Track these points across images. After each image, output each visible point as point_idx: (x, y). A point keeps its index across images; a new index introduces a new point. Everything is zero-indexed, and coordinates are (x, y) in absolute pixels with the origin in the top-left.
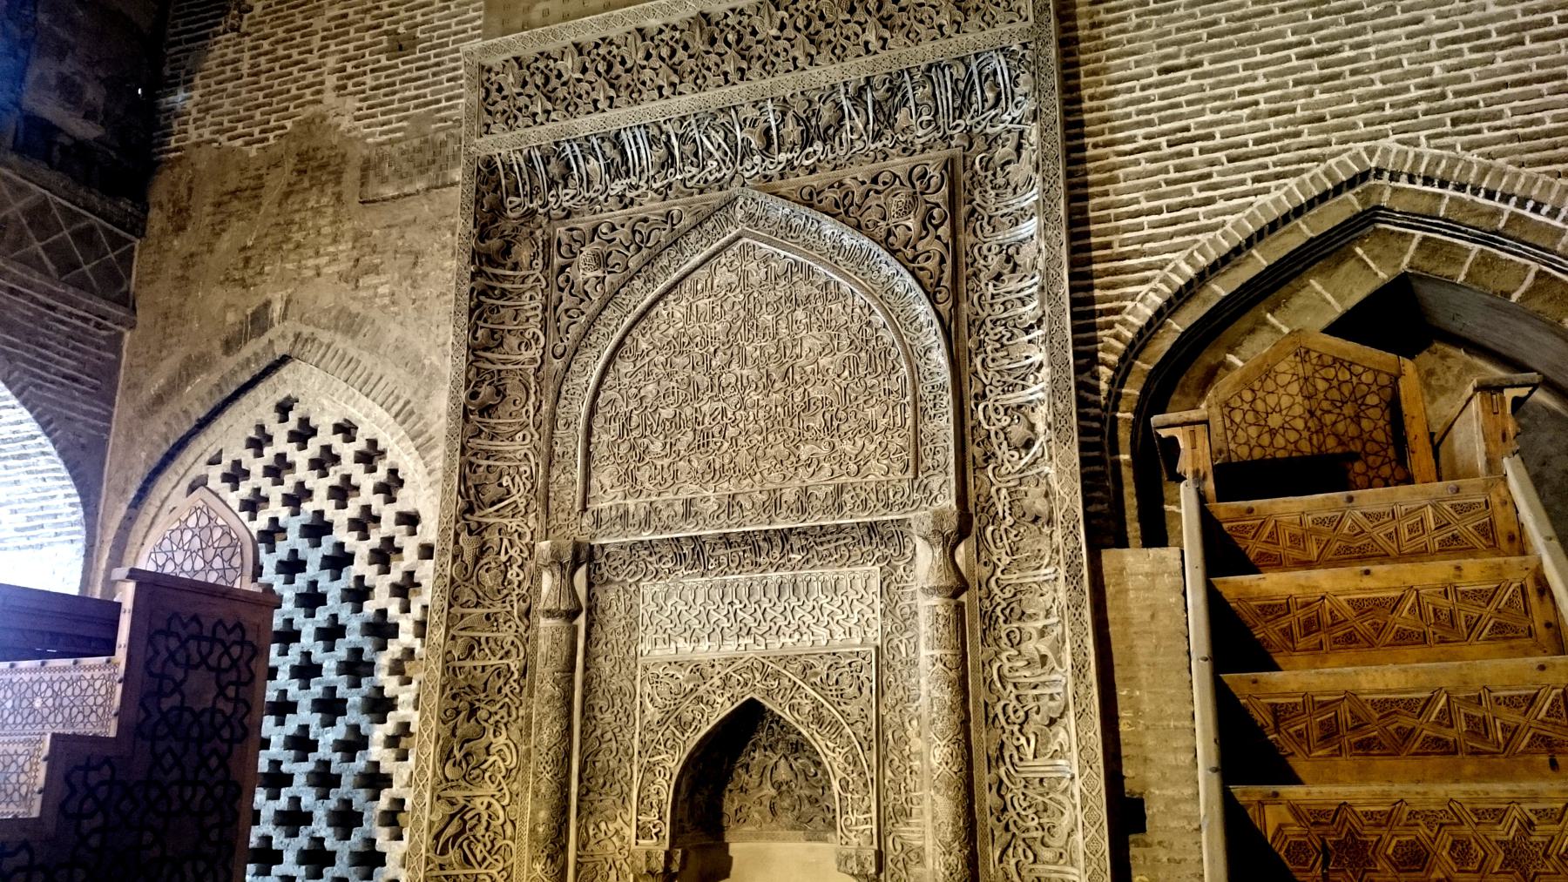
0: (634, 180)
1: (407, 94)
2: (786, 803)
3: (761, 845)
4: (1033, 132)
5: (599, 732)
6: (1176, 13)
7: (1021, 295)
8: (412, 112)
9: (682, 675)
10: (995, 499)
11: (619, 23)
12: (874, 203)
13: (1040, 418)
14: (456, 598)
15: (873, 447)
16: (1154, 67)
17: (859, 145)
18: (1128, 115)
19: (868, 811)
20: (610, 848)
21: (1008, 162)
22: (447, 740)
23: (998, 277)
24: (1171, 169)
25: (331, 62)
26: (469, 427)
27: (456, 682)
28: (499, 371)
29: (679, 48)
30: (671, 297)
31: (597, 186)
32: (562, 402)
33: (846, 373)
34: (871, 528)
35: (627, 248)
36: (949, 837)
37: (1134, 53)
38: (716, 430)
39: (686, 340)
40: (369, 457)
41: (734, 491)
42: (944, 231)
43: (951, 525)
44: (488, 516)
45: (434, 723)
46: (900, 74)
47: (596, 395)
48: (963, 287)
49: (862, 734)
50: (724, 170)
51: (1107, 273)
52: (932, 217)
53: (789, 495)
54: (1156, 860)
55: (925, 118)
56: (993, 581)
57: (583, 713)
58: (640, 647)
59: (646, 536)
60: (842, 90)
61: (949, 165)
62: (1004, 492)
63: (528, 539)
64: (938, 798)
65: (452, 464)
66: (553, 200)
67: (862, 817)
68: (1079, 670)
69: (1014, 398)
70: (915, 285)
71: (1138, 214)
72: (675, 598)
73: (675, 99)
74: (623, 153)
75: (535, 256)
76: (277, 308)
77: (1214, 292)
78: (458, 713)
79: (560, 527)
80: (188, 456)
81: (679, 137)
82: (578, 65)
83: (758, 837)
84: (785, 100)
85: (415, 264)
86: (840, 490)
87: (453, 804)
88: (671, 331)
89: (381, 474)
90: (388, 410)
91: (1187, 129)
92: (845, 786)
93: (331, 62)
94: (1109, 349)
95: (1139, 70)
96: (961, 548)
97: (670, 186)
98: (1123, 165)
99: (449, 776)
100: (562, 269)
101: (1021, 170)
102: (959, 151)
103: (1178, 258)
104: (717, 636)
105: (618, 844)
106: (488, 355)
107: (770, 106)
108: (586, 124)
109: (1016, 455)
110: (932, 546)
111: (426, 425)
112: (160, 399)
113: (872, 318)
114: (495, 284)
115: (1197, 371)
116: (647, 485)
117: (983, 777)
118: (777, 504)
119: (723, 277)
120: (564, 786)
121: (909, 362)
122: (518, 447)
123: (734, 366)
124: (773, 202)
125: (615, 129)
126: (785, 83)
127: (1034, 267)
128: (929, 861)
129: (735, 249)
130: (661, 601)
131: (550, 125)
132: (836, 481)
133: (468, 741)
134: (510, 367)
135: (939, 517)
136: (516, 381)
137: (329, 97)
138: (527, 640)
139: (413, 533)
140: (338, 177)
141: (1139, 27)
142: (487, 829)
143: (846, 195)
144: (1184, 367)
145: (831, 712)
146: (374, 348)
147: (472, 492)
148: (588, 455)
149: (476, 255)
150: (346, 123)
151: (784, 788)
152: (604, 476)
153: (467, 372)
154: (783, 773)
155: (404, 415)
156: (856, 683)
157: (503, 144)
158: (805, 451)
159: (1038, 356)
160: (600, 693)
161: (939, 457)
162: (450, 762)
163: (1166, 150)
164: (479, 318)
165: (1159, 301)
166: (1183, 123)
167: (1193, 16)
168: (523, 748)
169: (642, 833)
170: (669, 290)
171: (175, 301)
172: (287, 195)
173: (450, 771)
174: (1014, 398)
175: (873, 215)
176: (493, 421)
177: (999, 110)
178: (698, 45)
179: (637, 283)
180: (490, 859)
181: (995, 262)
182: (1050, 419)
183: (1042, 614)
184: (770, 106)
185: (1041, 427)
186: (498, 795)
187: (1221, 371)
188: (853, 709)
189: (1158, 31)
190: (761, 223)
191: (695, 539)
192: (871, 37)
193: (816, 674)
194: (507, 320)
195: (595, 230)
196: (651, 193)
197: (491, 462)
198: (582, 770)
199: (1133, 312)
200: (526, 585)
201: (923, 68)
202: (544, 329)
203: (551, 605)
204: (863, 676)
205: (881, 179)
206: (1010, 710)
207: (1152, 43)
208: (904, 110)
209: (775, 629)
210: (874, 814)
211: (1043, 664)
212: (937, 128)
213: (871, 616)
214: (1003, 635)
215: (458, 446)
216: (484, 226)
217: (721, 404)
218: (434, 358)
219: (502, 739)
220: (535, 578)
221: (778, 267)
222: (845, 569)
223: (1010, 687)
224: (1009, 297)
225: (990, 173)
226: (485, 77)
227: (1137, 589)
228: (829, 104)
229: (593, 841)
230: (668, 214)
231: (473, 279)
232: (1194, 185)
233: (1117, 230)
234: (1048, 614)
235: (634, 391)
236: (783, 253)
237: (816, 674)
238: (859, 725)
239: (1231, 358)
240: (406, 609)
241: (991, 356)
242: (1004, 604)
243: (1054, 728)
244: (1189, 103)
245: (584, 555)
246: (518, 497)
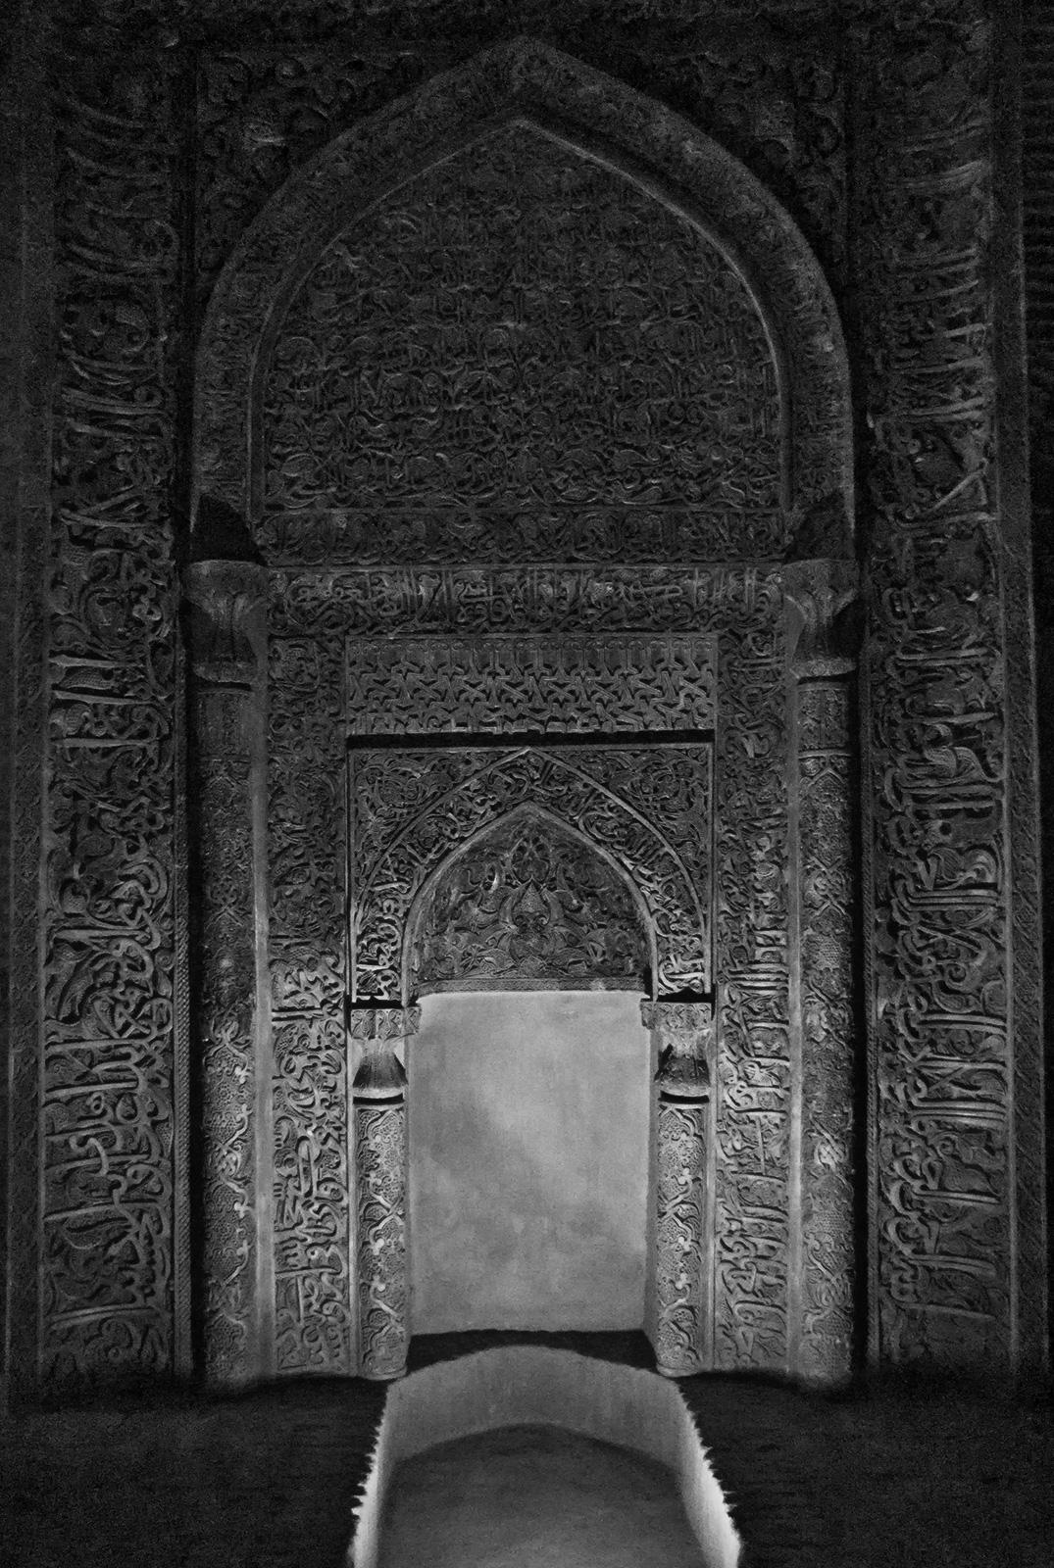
67: (689, 964)
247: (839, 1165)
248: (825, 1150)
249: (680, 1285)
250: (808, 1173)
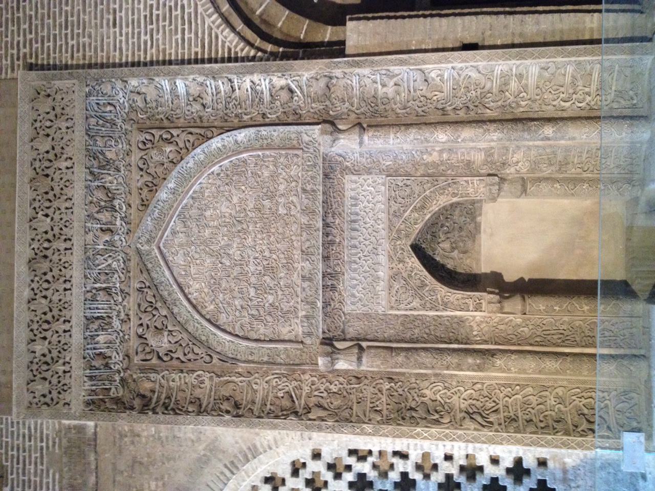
0: (115, 313)
1: (32, 471)
2: (461, 244)
3: (483, 259)
4: (134, 82)
5: (425, 336)
6: (87, 20)
7: (215, 94)
8: (44, 468)
9: (396, 286)
10: (316, 110)
11: (21, 314)
12: (154, 170)
13: (279, 82)
14: (347, 420)
15: (284, 174)
16: (112, 30)
17: (120, 180)
18: (133, 43)
19: (467, 182)
20: (486, 329)
21: (145, 100)
22: (429, 422)
23: (204, 106)
24: (164, 24)
26: (246, 415)
27: (395, 418)
28: (215, 400)
29: (44, 278)
30: (186, 291)
31: (114, 337)
32: (239, 357)
33: (243, 188)
34: (326, 176)
35: (154, 316)
36: (481, 130)
37: (103, 40)
38: (265, 263)
39: (212, 281)
41: (299, 252)
42: (175, 132)
43: (328, 127)
44: (300, 405)
45: (419, 429)
46: (87, 150)
47: (237, 336)
48: (206, 124)
49: (429, 185)
50: (120, 258)
51: (210, 50)
52: (166, 139)
53: (304, 220)
54: (490, 36)
55: (113, 143)
56: (357, 111)
57: (414, 343)
58: (380, 312)
59: (320, 304)
60: (89, 183)
61: (140, 130)
62: (313, 105)
63: (315, 379)
64: (462, 137)
65: (268, 424)
66: (117, 367)
67: (471, 185)
68: (402, 63)
69: (267, 97)
70: (201, 147)
71: (183, 39)
72: (355, 291)
73: (73, 280)
74: (98, 318)
75: (148, 379)
77: (226, 10)
78: (413, 417)
79: (311, 357)
81: (96, 282)
82: (41, 341)
83: (478, 261)
84: (88, 216)
85: (141, 463)
86: (304, 191)
87: (464, 418)
88: (206, 290)
90: (228, 480)
91: (145, 16)
92: (455, 195)
94: (249, 52)
95: (112, 38)
96: (340, 127)
97: (122, 291)
98: (158, 46)
99: (448, 420)
100: (159, 358)
101: (151, 94)
102: (135, 126)
103: (208, 21)
104: (376, 267)
105: (484, 325)
106: (204, 406)
107: (89, 225)
108: (77, 337)
109: (296, 98)
110: (338, 139)
111: (240, 452)
113: (215, 173)
114: (161, 403)
115: (263, 27)
116: (291, 304)
117: (452, 117)
118: (309, 227)
119: (179, 260)
120: (454, 350)
121: (241, 153)
123: (231, 252)
124: (142, 227)
125: (83, 319)
126: (79, 212)
127: (202, 84)
128: (493, 144)
129: (165, 251)
130: (356, 300)
131: (73, 362)
132: (300, 193)
133: (429, 411)
134: (213, 393)
135: (323, 132)
136: (222, 389)
138: (373, 377)
139: (304, 465)
141: (90, 37)
142: (478, 400)
143: (147, 186)
145: (417, 203)
147: (285, 413)
148: (271, 341)
149: (142, 411)
151: (454, 245)
152: (285, 331)
153: (213, 415)
154: (446, 245)
156: (404, 188)
157: (79, 390)
158: (282, 211)
159: (248, 84)
160: (404, 336)
161: (293, 136)
162: (440, 420)
163: (154, 26)
164: (181, 410)
165: (227, 30)
166: (142, 18)
167: (90, 12)
168: (433, 379)
169: (478, 308)
170: (182, 291)
173: (446, 420)
174: (267, 97)
175: (160, 170)
176: (244, 402)
177: (117, 105)
178: (45, 266)
179: (176, 310)
180: (494, 399)
181: (197, 107)
182: (280, 74)
183: (375, 85)
184: (89, 225)
185: (283, 82)
186: (459, 394)
187: (264, 17)
188: (417, 189)
189: (94, 28)
190: (153, 235)
191: (324, 276)
192: (64, 165)
193: (399, 209)
194: (184, 396)
195: (140, 337)
196: (125, 303)
197: (269, 403)
198: (446, 343)
199: (231, 42)
200: (341, 379)
201: (87, 138)
202: (193, 371)
203: (354, 358)
204: (400, 184)
205: (142, 166)
206: (420, 104)
207: (100, 30)
208: (107, 153)
209: (375, 233)
210: (469, 178)
211: (399, 85)
212: (120, 137)
213: (370, 181)
214: (384, 107)
215: (257, 420)
216: (125, 408)
217: (251, 260)
218: (201, 448)
219: (427, 392)
220: (339, 373)
222: (346, 194)
223: (410, 104)
224: (215, 101)
225: (149, 110)
226: (34, 406)
227: (365, 40)
228: (95, 192)
229: (484, 338)
230: (140, 290)
231: (157, 413)
232: (174, 13)
233: (190, 49)
234: (375, 82)
235: (237, 313)
236: (172, 223)
237: (399, 209)
238: (425, 186)
239: (258, 13)
240: (349, 468)
241: (244, 110)
242: (369, 107)
243: (430, 80)
244: (133, 14)
245: (328, 341)
246: (291, 386)
247: (553, 127)
248: (546, 132)
249: (603, 188)
250: (556, 139)
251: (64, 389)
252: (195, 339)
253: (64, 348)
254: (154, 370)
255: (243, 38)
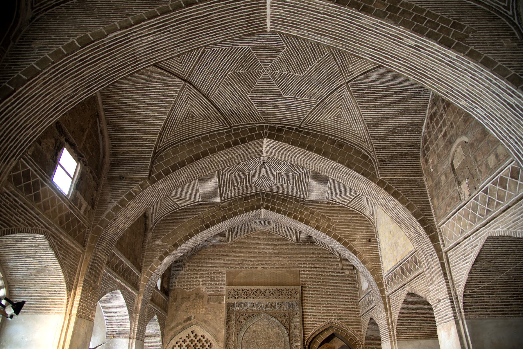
25: (201, 280)
40: (207, 341)
61: (289, 313)
69: (296, 344)
76: (193, 317)
80: (176, 337)
89: (209, 344)
93: (201, 280)
101: (297, 316)
108: (243, 300)
112: (173, 328)
115: (313, 341)
122: (232, 343)
137: (201, 286)
140: (202, 299)
144: (313, 341)
146: (209, 326)
150: (204, 290)
155: (214, 336)
157: (232, 301)
171: (175, 313)
172: (194, 299)
174: (296, 344)
221: (267, 323)
251: (232, 298)
252: (242, 327)
253: (241, 298)
254: (236, 317)
255: (309, 338)
